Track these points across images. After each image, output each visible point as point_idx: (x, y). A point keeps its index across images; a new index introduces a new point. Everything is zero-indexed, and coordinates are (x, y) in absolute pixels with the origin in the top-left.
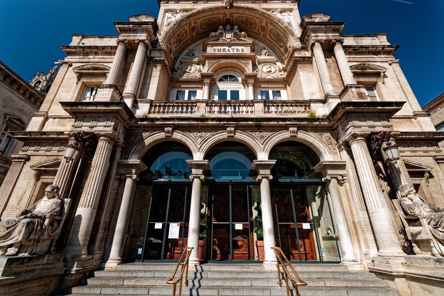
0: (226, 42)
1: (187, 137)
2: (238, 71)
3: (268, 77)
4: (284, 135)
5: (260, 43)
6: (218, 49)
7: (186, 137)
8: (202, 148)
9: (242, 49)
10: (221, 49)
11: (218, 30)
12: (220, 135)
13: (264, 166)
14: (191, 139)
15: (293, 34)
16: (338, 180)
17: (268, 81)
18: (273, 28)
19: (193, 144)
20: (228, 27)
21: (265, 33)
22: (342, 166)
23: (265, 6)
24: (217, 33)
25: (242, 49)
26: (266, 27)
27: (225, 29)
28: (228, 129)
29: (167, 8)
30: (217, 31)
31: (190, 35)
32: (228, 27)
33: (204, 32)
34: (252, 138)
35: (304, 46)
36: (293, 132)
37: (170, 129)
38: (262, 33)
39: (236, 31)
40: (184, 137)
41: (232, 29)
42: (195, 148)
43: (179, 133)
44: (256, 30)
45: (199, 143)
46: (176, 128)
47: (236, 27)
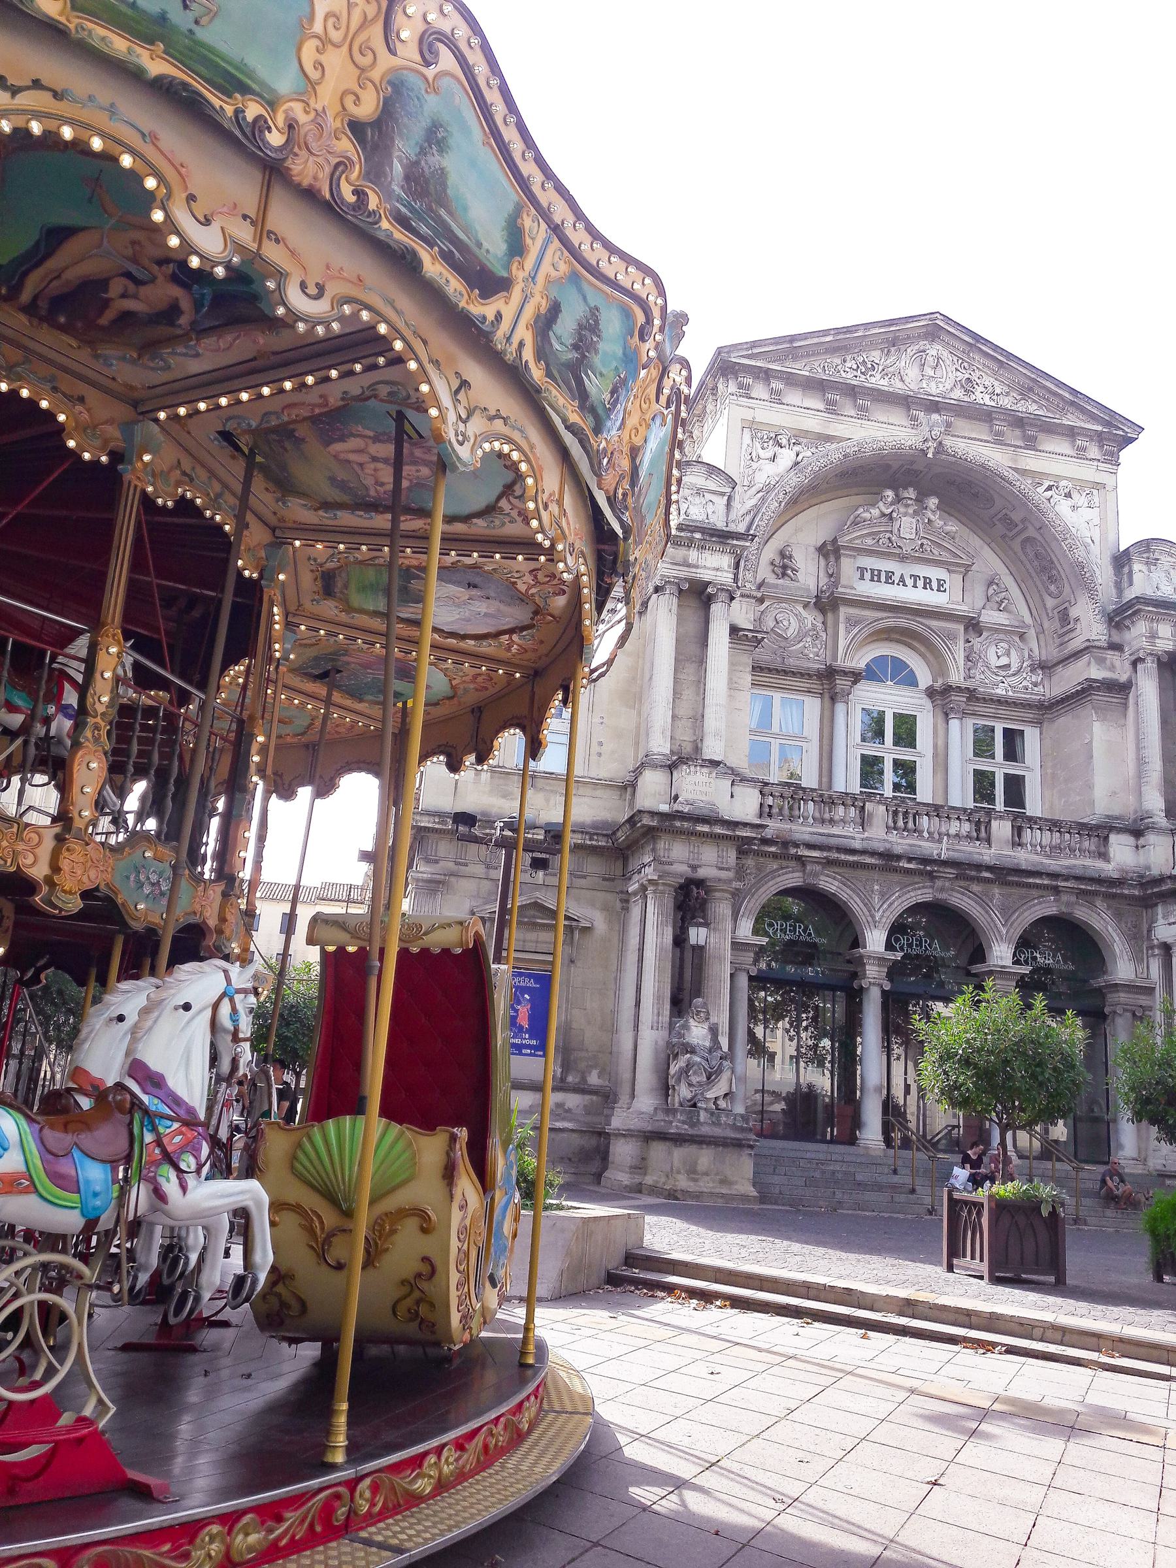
0: (897, 551)
1: (852, 890)
2: (923, 649)
3: (1000, 691)
4: (1048, 907)
5: (986, 547)
7: (848, 891)
8: (884, 920)
11: (881, 504)
12: (919, 892)
13: (1003, 974)
14: (860, 897)
15: (1090, 588)
16: (1134, 1014)
17: (999, 701)
18: (1040, 538)
19: (865, 910)
20: (911, 493)
22: (1150, 991)
23: (1031, 461)
24: (875, 512)
26: (1021, 526)
27: (898, 499)
28: (939, 883)
29: (748, 415)
30: (873, 505)
32: (911, 493)
34: (984, 909)
35: (1116, 639)
36: (1068, 904)
37: (818, 868)
38: (1000, 528)
39: (932, 517)
40: (844, 888)
42: (870, 919)
43: (834, 878)
45: (877, 908)
46: (830, 863)
47: (933, 502)
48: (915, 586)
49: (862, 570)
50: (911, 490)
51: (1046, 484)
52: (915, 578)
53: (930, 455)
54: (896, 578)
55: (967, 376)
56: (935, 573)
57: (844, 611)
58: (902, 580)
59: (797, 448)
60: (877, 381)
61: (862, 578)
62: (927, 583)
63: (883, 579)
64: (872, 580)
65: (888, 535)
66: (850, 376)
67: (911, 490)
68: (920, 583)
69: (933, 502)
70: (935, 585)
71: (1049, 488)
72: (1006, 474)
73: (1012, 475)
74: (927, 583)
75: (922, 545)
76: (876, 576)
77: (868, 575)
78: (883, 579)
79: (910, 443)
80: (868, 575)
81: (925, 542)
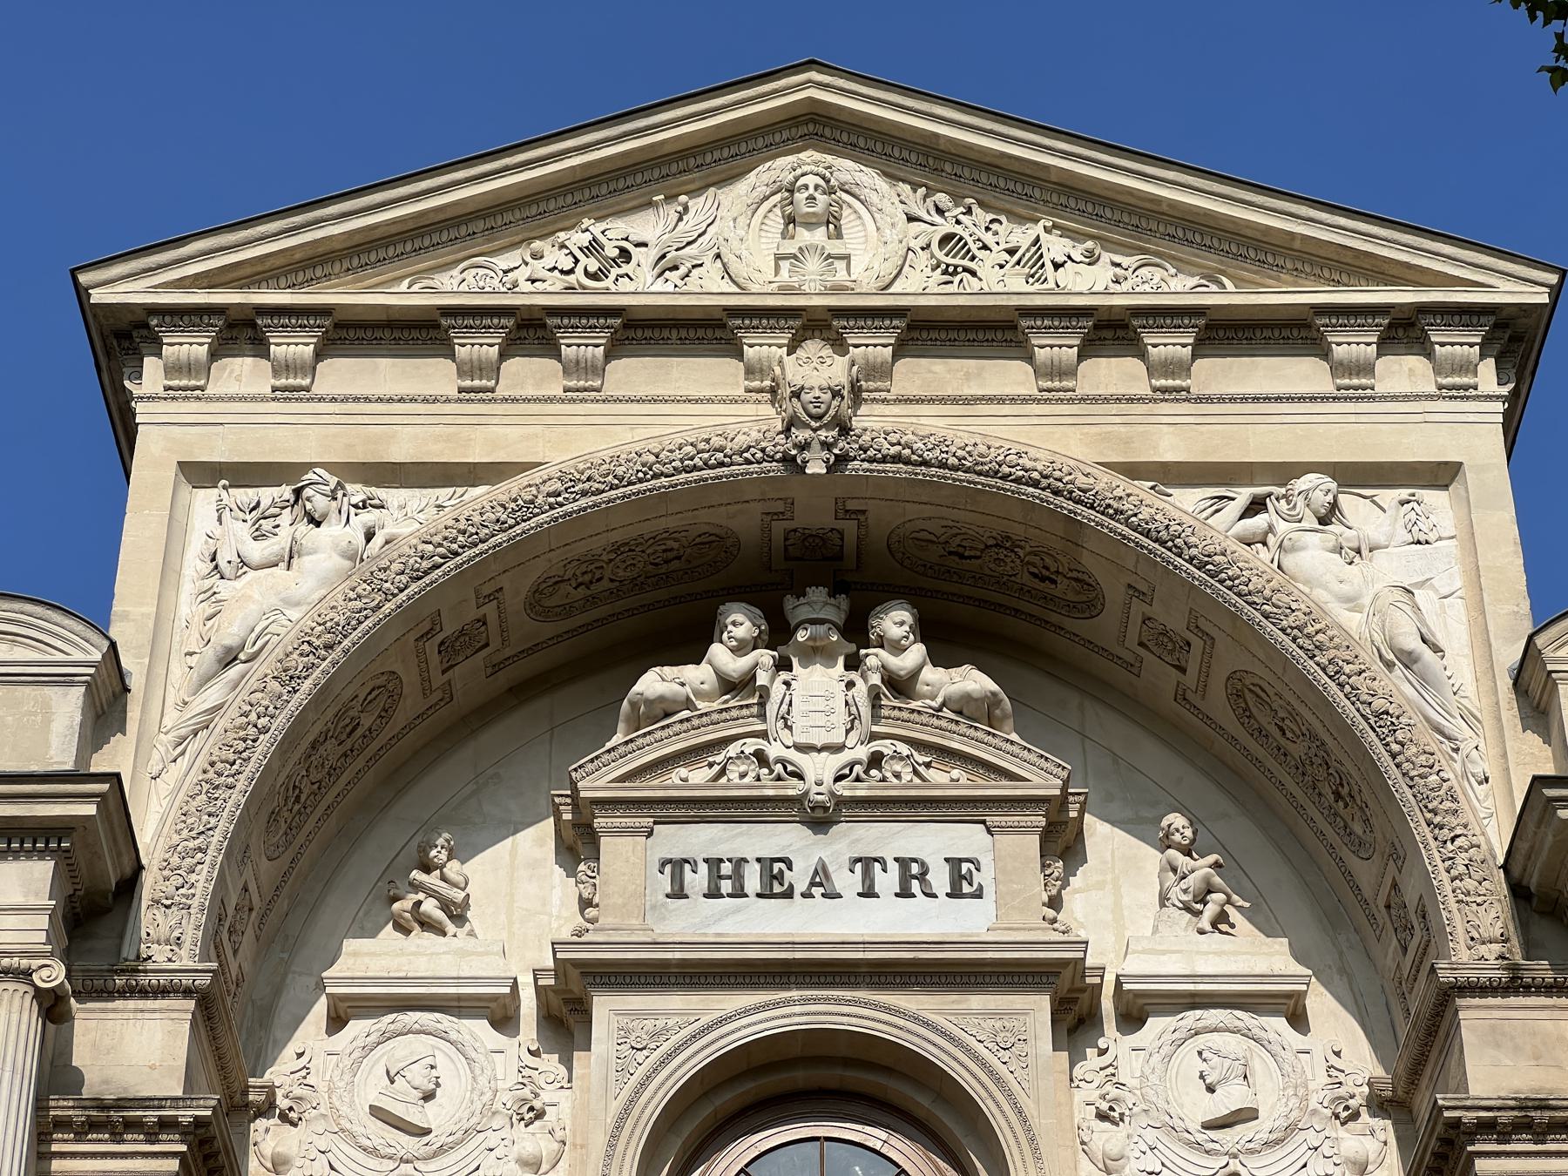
0: (793, 788)
6: (714, 863)
9: (954, 863)
10: (740, 863)
11: (718, 651)
20: (816, 609)
21: (1190, 679)
25: (954, 863)
27: (777, 633)
31: (426, 687)
32: (816, 609)
33: (557, 638)
41: (857, 631)
44: (1104, 627)
47: (895, 621)
48: (869, 893)
49: (677, 866)
50: (817, 594)
51: (1244, 495)
52: (867, 863)
53: (816, 468)
54: (799, 878)
55: (948, 227)
56: (933, 842)
57: (606, 1008)
58: (821, 878)
59: (368, 517)
60: (641, 287)
61: (678, 893)
62: (912, 877)
63: (753, 882)
64: (714, 893)
65: (751, 745)
66: (556, 282)
67: (817, 594)
68: (887, 881)
69: (895, 621)
70: (940, 879)
71: (1256, 506)
72: (1082, 481)
73: (1105, 482)
74: (912, 877)
75: (876, 760)
76: (724, 879)
77: (697, 880)
78: (753, 882)
79: (742, 441)
80: (697, 880)
81: (885, 747)
